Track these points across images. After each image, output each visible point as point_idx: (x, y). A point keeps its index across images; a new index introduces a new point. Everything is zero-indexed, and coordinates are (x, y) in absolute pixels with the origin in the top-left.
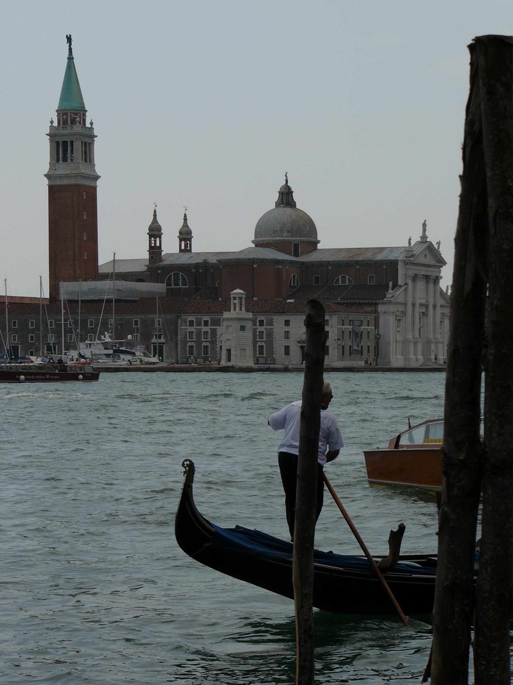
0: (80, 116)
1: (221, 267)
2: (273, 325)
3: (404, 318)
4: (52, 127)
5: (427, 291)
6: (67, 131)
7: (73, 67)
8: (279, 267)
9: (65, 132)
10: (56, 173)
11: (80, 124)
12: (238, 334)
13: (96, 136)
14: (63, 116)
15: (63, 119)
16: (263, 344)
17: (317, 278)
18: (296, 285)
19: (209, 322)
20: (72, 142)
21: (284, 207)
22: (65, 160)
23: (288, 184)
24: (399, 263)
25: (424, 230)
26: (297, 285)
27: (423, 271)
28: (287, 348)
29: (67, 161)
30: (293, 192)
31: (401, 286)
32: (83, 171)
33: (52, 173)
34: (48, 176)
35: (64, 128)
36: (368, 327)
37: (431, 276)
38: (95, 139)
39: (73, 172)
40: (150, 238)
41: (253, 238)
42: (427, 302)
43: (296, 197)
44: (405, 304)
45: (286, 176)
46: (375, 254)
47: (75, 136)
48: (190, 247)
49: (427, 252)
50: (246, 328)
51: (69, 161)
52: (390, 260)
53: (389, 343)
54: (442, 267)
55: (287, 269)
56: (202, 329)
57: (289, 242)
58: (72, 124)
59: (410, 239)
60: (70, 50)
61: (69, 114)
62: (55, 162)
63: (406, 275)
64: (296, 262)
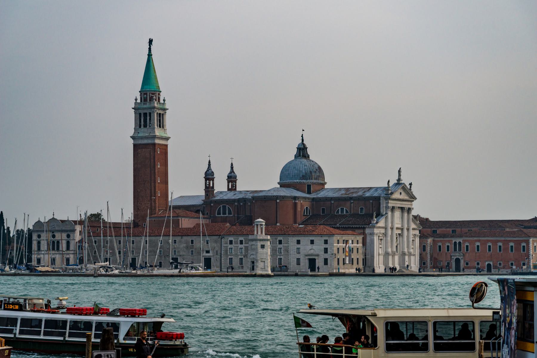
0: (156, 95)
1: (254, 202)
2: (288, 244)
3: (385, 238)
4: (136, 103)
6: (148, 105)
7: (151, 61)
8: (295, 202)
9: (145, 106)
10: (139, 135)
11: (156, 101)
14: (144, 95)
15: (144, 97)
16: (282, 257)
17: (323, 209)
18: (308, 214)
19: (244, 242)
20: (150, 114)
21: (301, 158)
22: (145, 126)
23: (304, 142)
25: (400, 175)
26: (309, 214)
28: (298, 260)
29: (146, 127)
31: (382, 215)
33: (136, 136)
35: (145, 104)
37: (404, 208)
38: (167, 111)
39: (151, 135)
40: (206, 181)
41: (279, 181)
42: (402, 227)
43: (309, 151)
44: (386, 228)
45: (302, 136)
46: (364, 192)
47: (153, 110)
48: (236, 187)
49: (402, 191)
51: (148, 127)
52: (375, 197)
53: (373, 256)
54: (413, 201)
55: (301, 203)
56: (239, 246)
57: (304, 184)
58: (150, 100)
59: (389, 182)
60: (150, 49)
61: (148, 94)
62: (138, 127)
63: (386, 207)
64: (308, 198)
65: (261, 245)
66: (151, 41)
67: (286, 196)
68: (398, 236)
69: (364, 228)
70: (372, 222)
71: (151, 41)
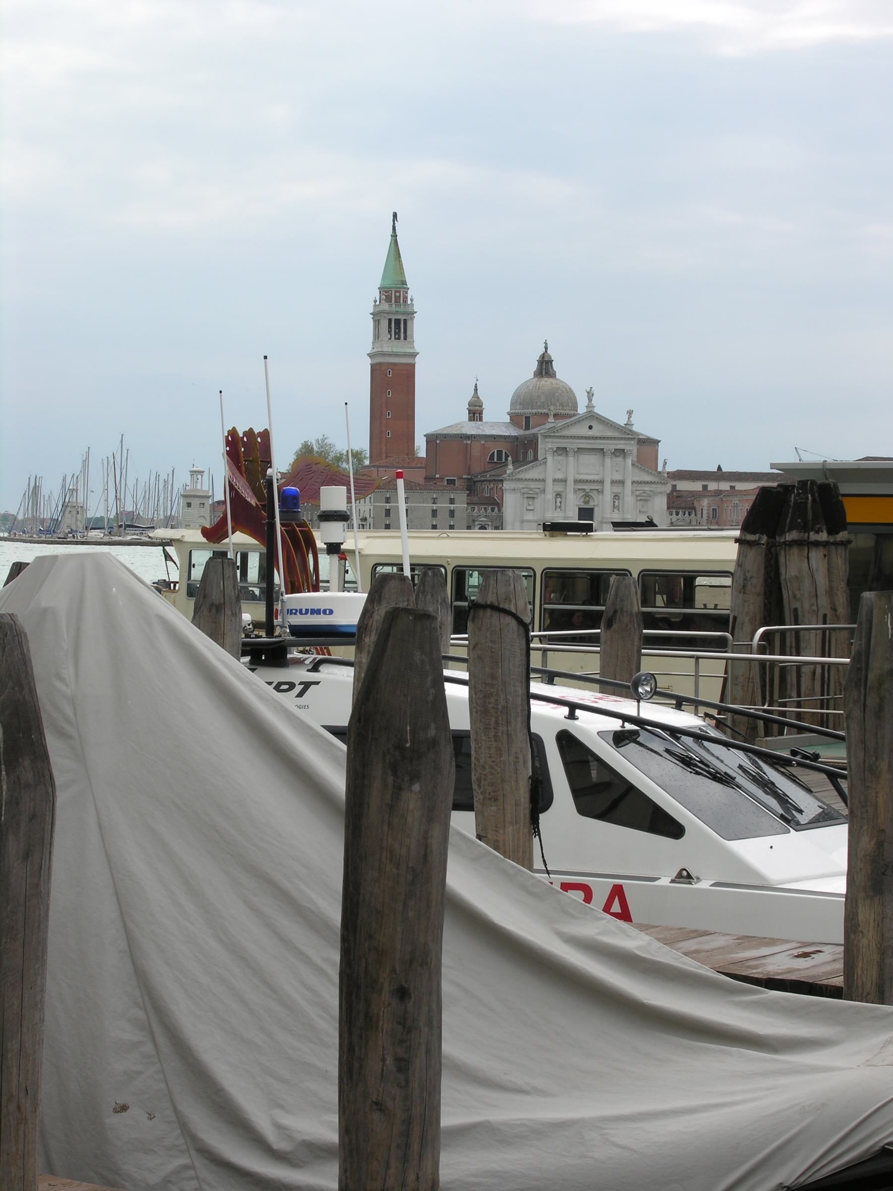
4: (375, 306)
5: (603, 465)
12: (184, 510)
13: (416, 312)
24: (539, 435)
25: (590, 400)
27: (584, 444)
30: (553, 361)
31: (539, 461)
32: (386, 349)
34: (371, 356)
36: (452, 506)
38: (414, 315)
44: (544, 480)
45: (546, 343)
49: (595, 424)
50: (192, 505)
55: (482, 444)
64: (505, 437)
65: (188, 503)
66: (395, 215)
67: (448, 435)
68: (595, 492)
69: (502, 481)
70: (508, 472)
71: (395, 215)
